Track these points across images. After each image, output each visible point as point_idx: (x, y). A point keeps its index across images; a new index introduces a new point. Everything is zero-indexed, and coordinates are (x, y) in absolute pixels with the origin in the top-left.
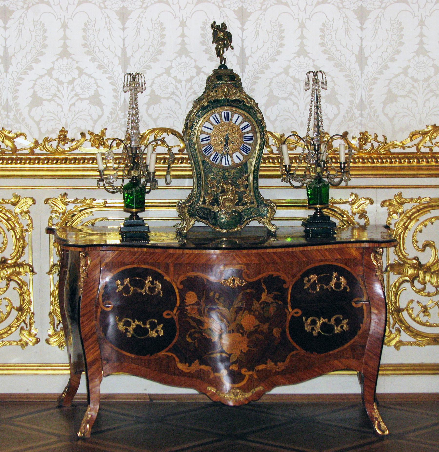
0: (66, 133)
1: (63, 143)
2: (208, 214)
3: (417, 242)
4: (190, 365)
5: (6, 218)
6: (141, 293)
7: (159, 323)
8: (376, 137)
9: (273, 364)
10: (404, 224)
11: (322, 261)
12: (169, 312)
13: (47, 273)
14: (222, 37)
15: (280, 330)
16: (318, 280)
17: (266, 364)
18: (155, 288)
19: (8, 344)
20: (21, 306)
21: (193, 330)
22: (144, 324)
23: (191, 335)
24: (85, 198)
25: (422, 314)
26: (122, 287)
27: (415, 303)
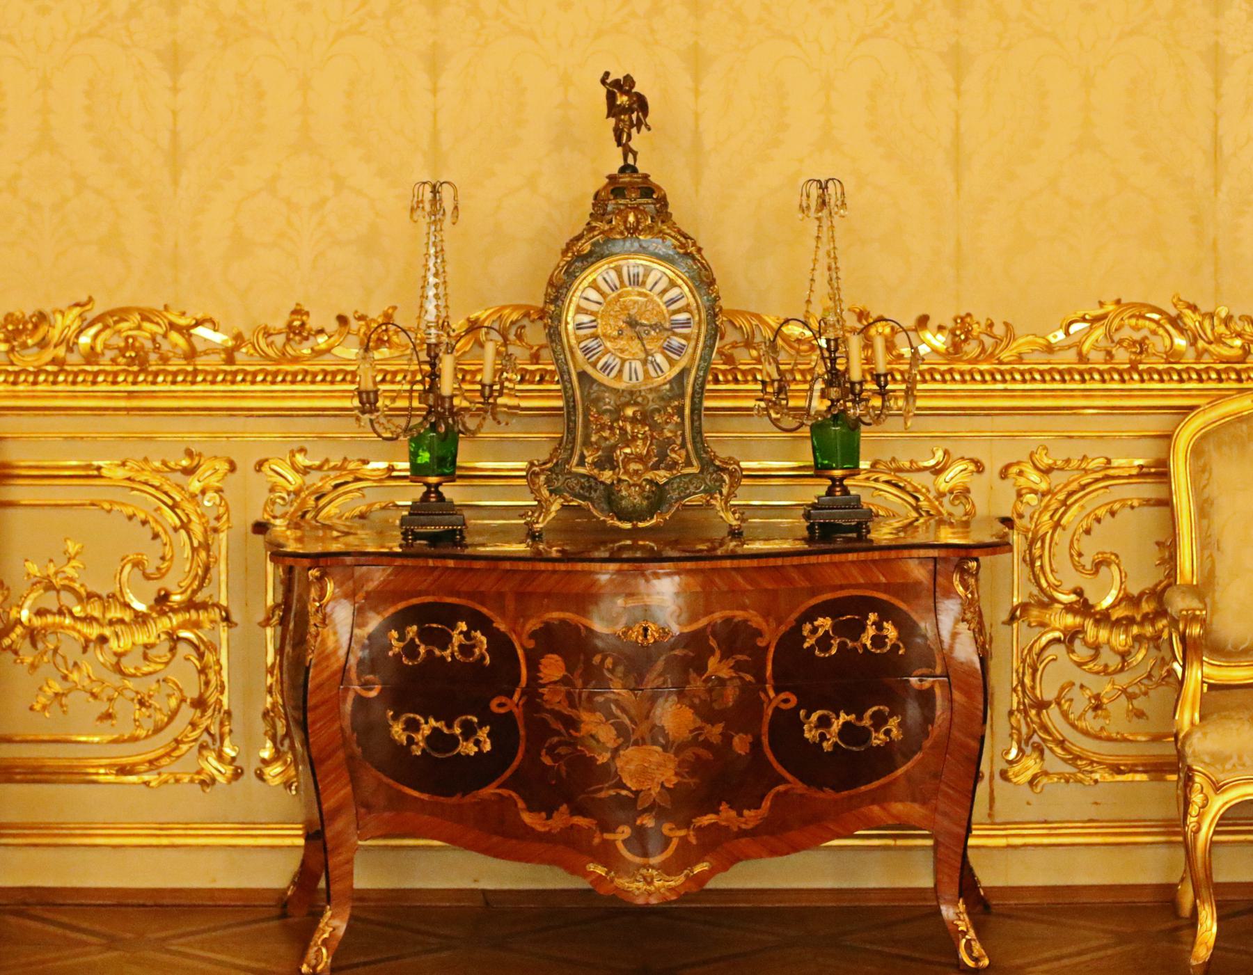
0: (305, 318)
1: (297, 338)
2: (590, 487)
3: (1080, 555)
4: (549, 817)
5: (170, 502)
6: (443, 658)
7: (481, 724)
8: (991, 325)
9: (733, 813)
10: (1052, 517)
11: (842, 587)
12: (504, 699)
13: (260, 624)
14: (626, 105)
15: (750, 738)
16: (834, 627)
17: (717, 812)
18: (474, 646)
19: (172, 781)
20: (201, 695)
21: (556, 739)
22: (450, 726)
23: (551, 751)
24: (345, 459)
25: (1090, 714)
26: (402, 644)
27: (1077, 688)
